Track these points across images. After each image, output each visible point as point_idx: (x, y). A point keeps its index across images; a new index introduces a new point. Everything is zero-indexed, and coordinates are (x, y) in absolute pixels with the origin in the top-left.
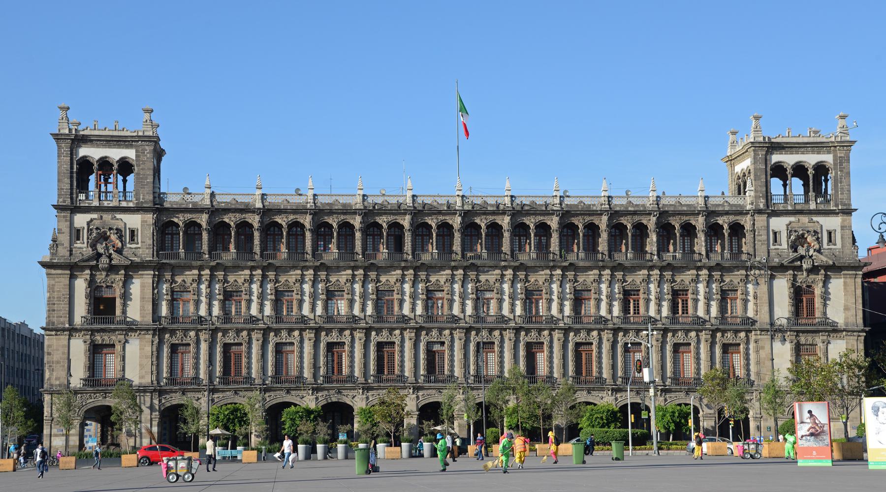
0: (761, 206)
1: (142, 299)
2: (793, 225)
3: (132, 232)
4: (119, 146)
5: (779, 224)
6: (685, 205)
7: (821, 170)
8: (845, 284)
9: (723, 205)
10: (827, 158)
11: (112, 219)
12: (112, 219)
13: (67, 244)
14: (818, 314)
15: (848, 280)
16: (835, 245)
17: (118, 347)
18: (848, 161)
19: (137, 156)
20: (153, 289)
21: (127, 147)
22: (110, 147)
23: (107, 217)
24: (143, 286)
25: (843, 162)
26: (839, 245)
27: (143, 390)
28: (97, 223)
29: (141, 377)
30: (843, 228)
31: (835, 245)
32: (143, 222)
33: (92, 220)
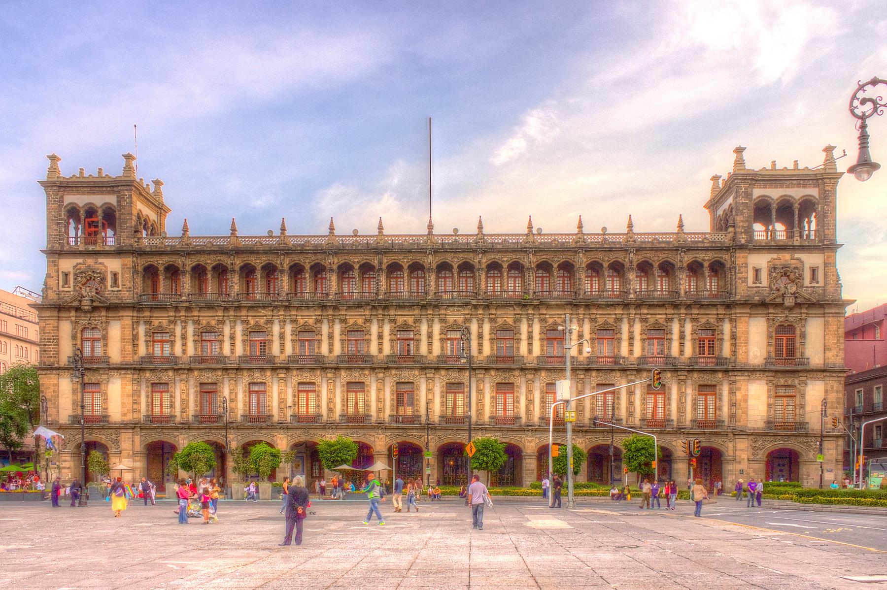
0: (743, 241)
1: (123, 339)
2: (777, 262)
3: (115, 275)
4: (102, 193)
5: (761, 261)
6: (663, 242)
7: (807, 206)
8: (826, 324)
9: (702, 242)
10: (814, 192)
11: (96, 263)
12: (96, 263)
13: (55, 289)
14: (798, 355)
15: (830, 319)
16: (818, 282)
17: (103, 387)
18: (835, 194)
19: (119, 202)
20: (133, 329)
21: (109, 193)
22: (94, 193)
23: (90, 261)
24: (123, 328)
25: (828, 197)
26: (821, 283)
27: (125, 426)
28: (83, 267)
29: (124, 415)
30: (826, 265)
31: (818, 282)
32: (123, 265)
33: (78, 264)
